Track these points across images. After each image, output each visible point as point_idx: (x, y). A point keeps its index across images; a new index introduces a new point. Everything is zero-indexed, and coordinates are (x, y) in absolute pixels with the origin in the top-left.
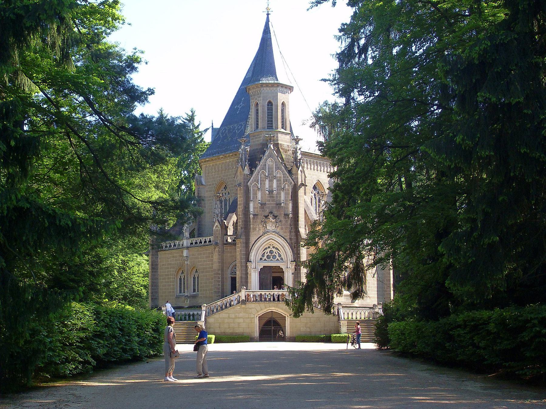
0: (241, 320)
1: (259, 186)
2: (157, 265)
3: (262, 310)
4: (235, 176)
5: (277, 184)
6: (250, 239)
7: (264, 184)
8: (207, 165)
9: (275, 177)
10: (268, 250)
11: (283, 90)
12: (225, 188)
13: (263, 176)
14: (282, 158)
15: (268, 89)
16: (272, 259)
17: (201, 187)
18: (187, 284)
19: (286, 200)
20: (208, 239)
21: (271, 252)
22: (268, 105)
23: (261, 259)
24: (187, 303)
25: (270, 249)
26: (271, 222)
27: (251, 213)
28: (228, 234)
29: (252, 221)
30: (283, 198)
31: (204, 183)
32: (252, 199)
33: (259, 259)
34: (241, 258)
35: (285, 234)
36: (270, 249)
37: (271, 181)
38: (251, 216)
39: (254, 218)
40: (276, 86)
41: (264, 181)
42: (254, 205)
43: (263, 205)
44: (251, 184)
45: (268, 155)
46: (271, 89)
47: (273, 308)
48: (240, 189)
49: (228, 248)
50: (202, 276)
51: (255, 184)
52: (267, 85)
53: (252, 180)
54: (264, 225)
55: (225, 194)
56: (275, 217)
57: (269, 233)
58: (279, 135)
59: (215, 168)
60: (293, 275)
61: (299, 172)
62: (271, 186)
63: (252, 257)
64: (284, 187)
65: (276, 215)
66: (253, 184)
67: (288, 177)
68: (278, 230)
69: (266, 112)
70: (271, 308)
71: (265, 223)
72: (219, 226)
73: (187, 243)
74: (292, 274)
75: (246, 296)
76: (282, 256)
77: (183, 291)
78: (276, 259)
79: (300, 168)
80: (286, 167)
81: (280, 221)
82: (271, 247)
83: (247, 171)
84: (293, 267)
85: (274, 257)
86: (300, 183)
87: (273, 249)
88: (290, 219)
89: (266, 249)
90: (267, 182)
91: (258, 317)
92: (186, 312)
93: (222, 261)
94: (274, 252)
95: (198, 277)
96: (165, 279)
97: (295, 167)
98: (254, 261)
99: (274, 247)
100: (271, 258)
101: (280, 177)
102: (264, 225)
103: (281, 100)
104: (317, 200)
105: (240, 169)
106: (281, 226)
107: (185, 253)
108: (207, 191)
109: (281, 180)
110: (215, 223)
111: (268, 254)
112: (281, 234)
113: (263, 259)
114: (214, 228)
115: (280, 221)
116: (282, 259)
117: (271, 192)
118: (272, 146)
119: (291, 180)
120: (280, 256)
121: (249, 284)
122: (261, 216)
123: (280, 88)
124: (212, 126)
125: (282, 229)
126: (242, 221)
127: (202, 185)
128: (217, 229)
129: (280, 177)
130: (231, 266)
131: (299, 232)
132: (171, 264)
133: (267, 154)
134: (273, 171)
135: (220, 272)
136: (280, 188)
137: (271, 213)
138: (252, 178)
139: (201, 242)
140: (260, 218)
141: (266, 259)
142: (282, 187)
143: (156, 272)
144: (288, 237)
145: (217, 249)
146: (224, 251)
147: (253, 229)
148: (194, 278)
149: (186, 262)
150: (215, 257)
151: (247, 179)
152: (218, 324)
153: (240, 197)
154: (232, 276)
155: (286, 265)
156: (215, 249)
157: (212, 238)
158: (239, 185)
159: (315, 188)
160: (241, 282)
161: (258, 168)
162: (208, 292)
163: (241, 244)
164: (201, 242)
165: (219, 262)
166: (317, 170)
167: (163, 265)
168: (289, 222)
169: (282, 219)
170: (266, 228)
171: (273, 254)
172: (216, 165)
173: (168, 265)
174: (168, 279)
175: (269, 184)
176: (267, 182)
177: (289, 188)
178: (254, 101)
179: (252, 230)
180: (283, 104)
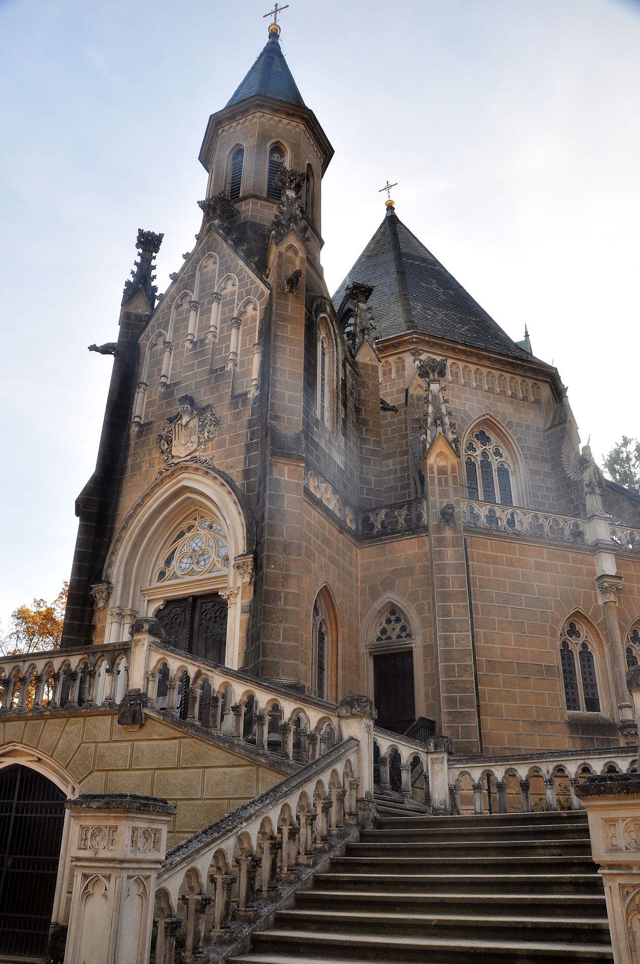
9: (217, 297)
19: (246, 352)
27: (137, 419)
29: (132, 443)
38: (134, 429)
39: (140, 434)
62: (204, 327)
88: (251, 402)
144: (240, 468)
168: (247, 415)
169: (224, 412)
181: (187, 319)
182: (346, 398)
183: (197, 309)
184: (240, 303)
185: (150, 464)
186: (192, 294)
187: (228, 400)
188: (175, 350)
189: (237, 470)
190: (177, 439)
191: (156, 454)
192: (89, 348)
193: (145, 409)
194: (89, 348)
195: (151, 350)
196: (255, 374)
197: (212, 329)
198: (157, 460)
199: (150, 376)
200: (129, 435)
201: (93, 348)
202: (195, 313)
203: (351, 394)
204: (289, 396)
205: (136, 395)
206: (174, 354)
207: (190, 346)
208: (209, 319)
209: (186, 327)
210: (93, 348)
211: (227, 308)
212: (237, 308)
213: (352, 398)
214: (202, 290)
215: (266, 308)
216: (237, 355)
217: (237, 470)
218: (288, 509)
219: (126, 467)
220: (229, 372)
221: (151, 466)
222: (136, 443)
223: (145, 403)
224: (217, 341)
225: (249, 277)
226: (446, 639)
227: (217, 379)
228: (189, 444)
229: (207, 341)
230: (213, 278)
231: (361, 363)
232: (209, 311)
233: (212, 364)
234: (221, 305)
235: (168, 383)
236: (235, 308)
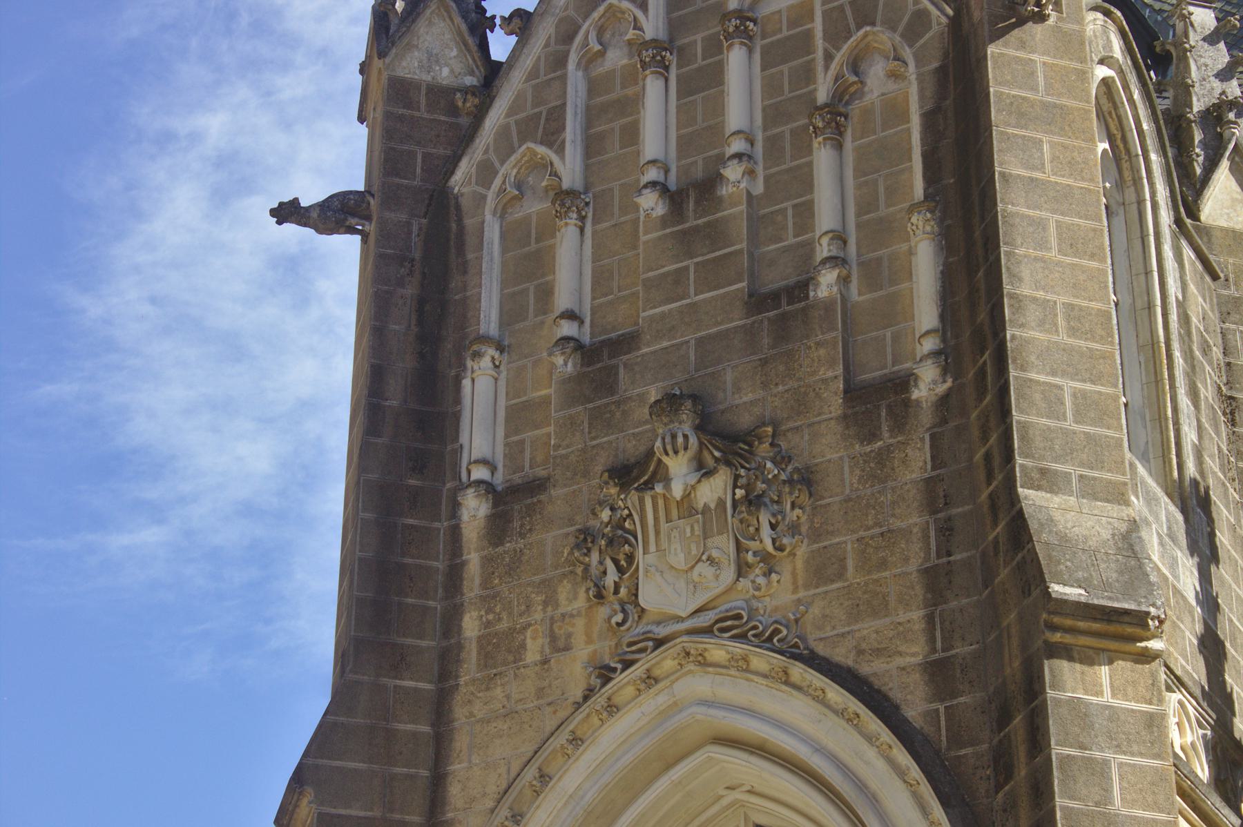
1: (570, 169)
26: (687, 507)
27: (480, 473)
29: (473, 560)
35: (868, 628)
38: (474, 509)
39: (498, 527)
44: (486, 172)
53: (503, 133)
54: (612, 576)
57: (666, 661)
64: (842, 97)
66: (508, 170)
81: (807, 479)
88: (926, 418)
122: (586, 474)
144: (915, 652)
147: (487, 658)
175: (685, 114)
179: (469, 668)
181: (631, 105)
182: (1193, 367)
183: (667, 68)
184: (838, 49)
185: (553, 638)
186: (639, 14)
187: (834, 404)
188: (595, 222)
189: (900, 661)
190: (652, 548)
192: (273, 212)
193: (506, 436)
194: (273, 212)
195: (502, 217)
196: (926, 314)
197: (737, 146)
198: (580, 623)
199: (512, 314)
200: (455, 533)
201: (287, 212)
202: (660, 83)
203: (1206, 350)
204: (1074, 395)
205: (466, 383)
206: (594, 233)
207: (660, 210)
208: (717, 107)
209: (632, 135)
210: (287, 212)
211: (785, 68)
212: (827, 68)
213: (1210, 363)
215: (942, 71)
216: (845, 242)
217: (900, 661)
218: (1124, 811)
219: (460, 647)
220: (828, 306)
221: (559, 645)
222: (487, 561)
223: (501, 414)
224: (759, 188)
227: (783, 331)
228: (704, 569)
229: (724, 191)
231: (1222, 229)
232: (715, 76)
233: (752, 275)
234: (757, 56)
235: (586, 339)
236: (820, 68)
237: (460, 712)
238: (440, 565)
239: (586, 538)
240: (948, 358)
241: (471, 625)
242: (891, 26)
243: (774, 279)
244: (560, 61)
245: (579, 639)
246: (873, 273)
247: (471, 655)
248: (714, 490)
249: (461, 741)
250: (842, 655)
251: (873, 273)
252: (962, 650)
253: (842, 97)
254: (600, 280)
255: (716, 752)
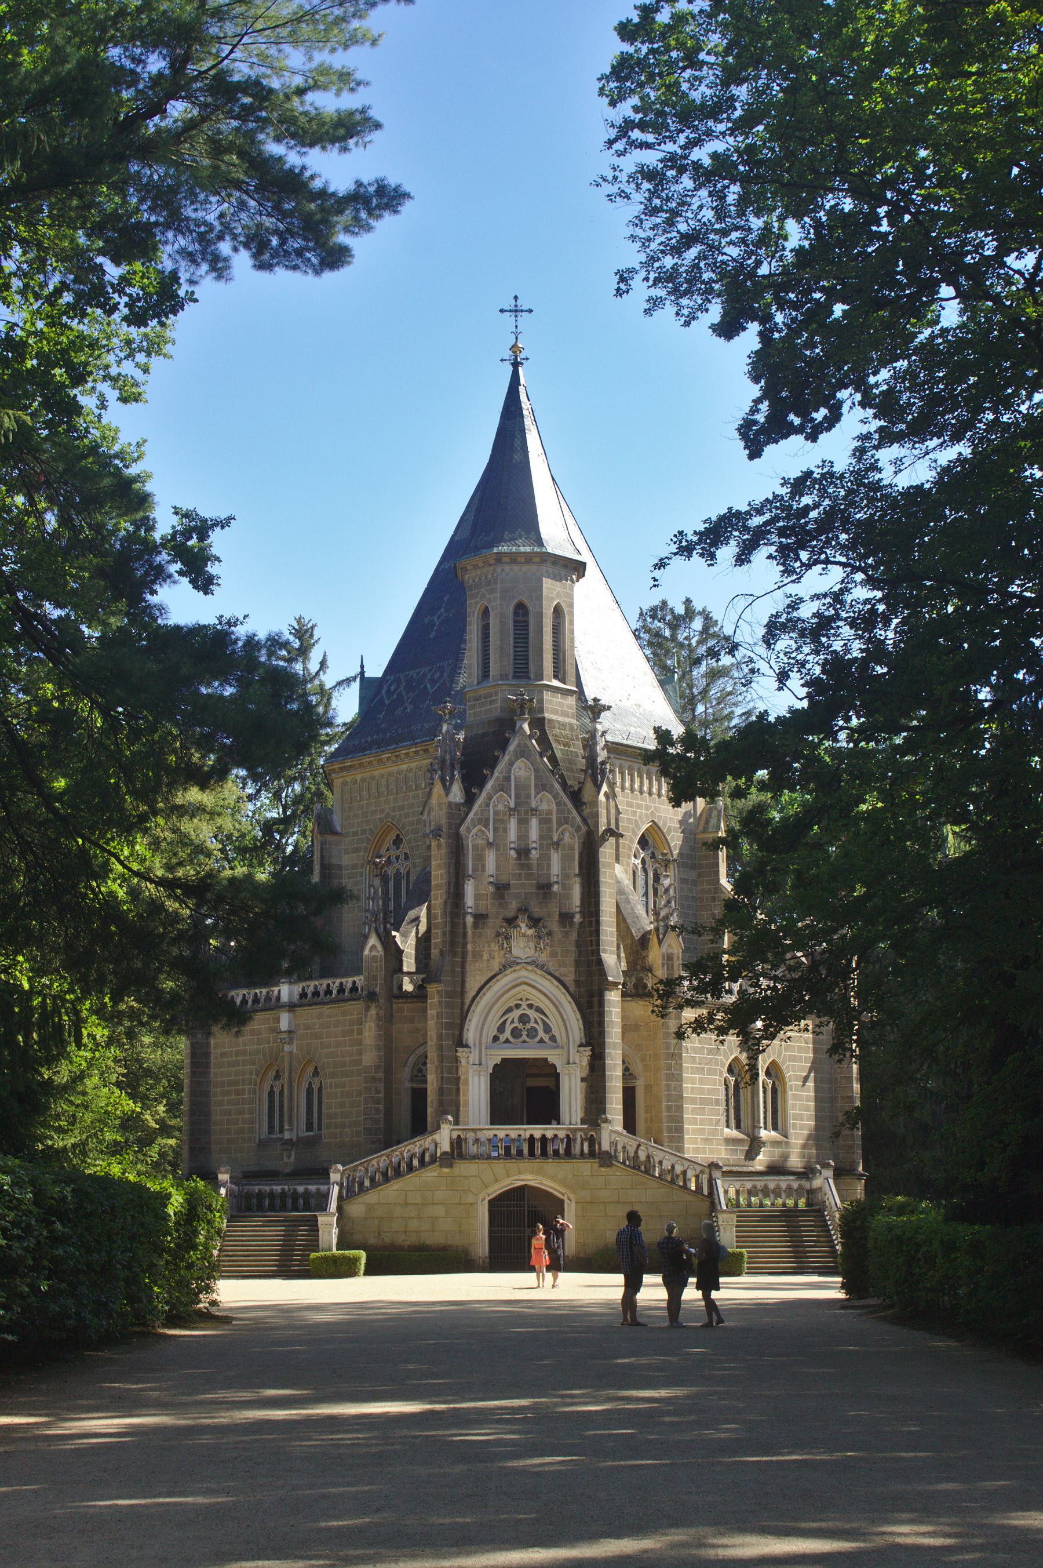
0: (439, 1211)
2: (207, 1055)
3: (497, 1181)
4: (423, 810)
5: (541, 830)
6: (467, 985)
7: (505, 830)
8: (349, 779)
9: (534, 811)
10: (516, 1014)
11: (556, 572)
12: (397, 842)
13: (501, 807)
14: (553, 759)
15: (516, 568)
16: (527, 1039)
17: (330, 838)
18: (291, 1109)
19: (565, 876)
20: (348, 982)
21: (524, 1019)
22: (516, 613)
23: (496, 1039)
24: (290, 1160)
25: (519, 1012)
26: (524, 935)
28: (405, 969)
29: (470, 932)
30: (555, 868)
31: (338, 828)
32: (470, 873)
33: (491, 1038)
34: (440, 1037)
35: (562, 970)
36: (519, 1012)
37: (523, 823)
38: (469, 920)
39: (476, 925)
40: (538, 560)
41: (503, 821)
42: (476, 888)
43: (501, 889)
44: (469, 831)
45: (515, 751)
46: (525, 568)
47: (530, 1177)
48: (439, 846)
49: (406, 1008)
50: (331, 1086)
51: (480, 830)
52: (513, 558)
53: (473, 820)
55: (397, 858)
56: (535, 922)
57: (518, 968)
58: (547, 696)
59: (369, 789)
60: (584, 1084)
61: (602, 797)
62: (523, 836)
63: (471, 1034)
64: (560, 840)
65: (536, 916)
66: (475, 831)
67: (569, 812)
68: (543, 958)
69: (511, 632)
70: (523, 1177)
71: (507, 938)
72: (379, 948)
73: (291, 994)
74: (583, 1080)
75: (451, 1143)
76: (555, 1031)
77: (277, 1128)
78: (538, 1039)
79: (605, 788)
80: (564, 785)
81: (550, 934)
82: (524, 1006)
83: (457, 794)
84: (585, 1061)
85: (532, 1033)
86: (602, 828)
87: (532, 1014)
88: (577, 926)
89: (509, 1010)
90: (513, 825)
91: (486, 1202)
92: (286, 1187)
93: (387, 1045)
94: (532, 1020)
95: (320, 1089)
96: (229, 1093)
97: (589, 786)
98: (475, 1045)
99: (530, 1006)
100: (524, 1037)
101: (550, 813)
102: (505, 945)
103: (553, 599)
104: (651, 875)
105: (438, 788)
106: (552, 946)
107: (285, 1021)
108: (347, 852)
109: (549, 821)
110: (366, 937)
111: (514, 1025)
112: (551, 969)
113: (503, 1038)
114: (366, 952)
115: (550, 934)
116: (553, 1039)
117: (523, 852)
118: (526, 727)
119: (578, 819)
120: (547, 1029)
121: (461, 1109)
123: (548, 568)
124: (362, 673)
125: (553, 954)
126: (444, 934)
127: (335, 833)
128: (374, 953)
129: (550, 813)
130: (412, 1059)
131: (600, 962)
132: (244, 1053)
133: (512, 748)
134: (528, 796)
135: (381, 1075)
136: (548, 843)
137: (523, 910)
138: (471, 815)
139: (328, 992)
140: (494, 923)
141: (511, 1039)
142: (555, 839)
143: (206, 1073)
145: (373, 1012)
146: (392, 1016)
147: (474, 956)
148: (310, 1092)
149: (287, 1048)
150: (367, 1033)
151: (459, 814)
152: (376, 1222)
153: (439, 866)
154: (415, 1086)
155: (565, 1054)
156: (368, 1009)
157: (359, 980)
158: (437, 833)
159: (643, 842)
160: (441, 1103)
161: (489, 785)
162: (347, 1130)
163: (441, 997)
164: (328, 992)
165: (378, 1048)
166: (650, 794)
167: (223, 1055)
168: (574, 936)
169: (554, 926)
170: (510, 951)
171: (528, 1026)
172: (373, 778)
173: (237, 1055)
174: (238, 1093)
175: (519, 829)
176: (513, 825)
177: (572, 840)
178: (476, 603)
180: (558, 611)
187: (557, 917)
191: (495, 947)
198: (496, 954)
200: (465, 924)
207: (515, 856)
214: (517, 796)
221: (492, 957)
222: (473, 933)
225: (565, 805)
226: (668, 1087)
228: (527, 949)
230: (528, 787)
237: (468, 967)
238: (461, 931)
239: (498, 934)
240: (583, 916)
241: (469, 947)
242: (572, 826)
243: (543, 881)
244: (488, 805)
245: (497, 957)
246: (564, 887)
247: (470, 955)
248: (530, 932)
249: (468, 974)
250: (556, 974)
251: (564, 887)
252: (582, 979)
253: (560, 840)
254: (498, 867)
255: (525, 987)
